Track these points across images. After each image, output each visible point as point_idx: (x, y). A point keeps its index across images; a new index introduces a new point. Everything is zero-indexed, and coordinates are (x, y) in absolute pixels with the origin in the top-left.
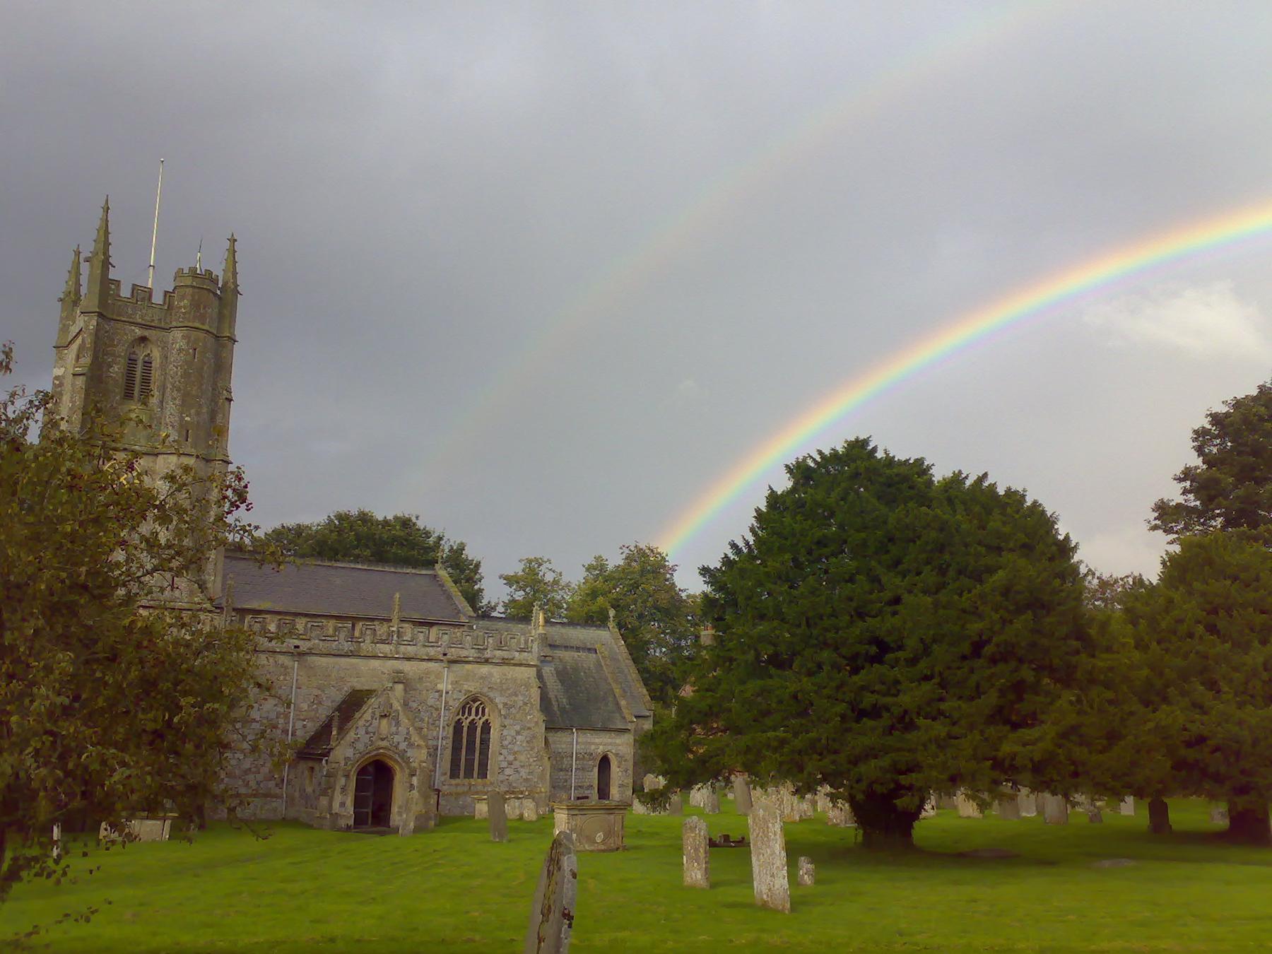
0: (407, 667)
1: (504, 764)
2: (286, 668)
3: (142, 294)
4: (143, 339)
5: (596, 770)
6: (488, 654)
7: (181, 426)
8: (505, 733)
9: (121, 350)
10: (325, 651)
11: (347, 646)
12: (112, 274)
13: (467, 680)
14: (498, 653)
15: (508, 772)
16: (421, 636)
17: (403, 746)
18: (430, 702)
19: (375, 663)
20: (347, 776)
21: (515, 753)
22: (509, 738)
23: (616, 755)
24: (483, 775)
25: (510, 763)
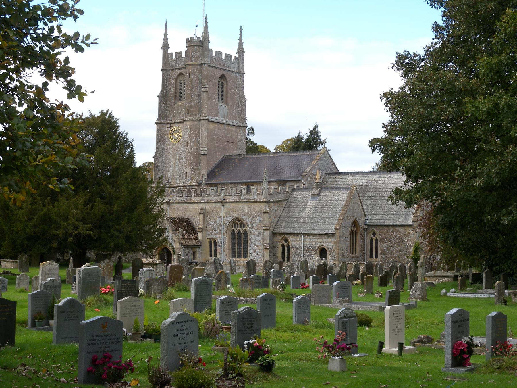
0: (208, 207)
1: (252, 251)
3: (179, 54)
4: (181, 74)
6: (243, 198)
8: (252, 236)
9: (173, 81)
12: (169, 51)
13: (232, 211)
14: (247, 197)
15: (254, 255)
16: (213, 192)
18: (218, 222)
19: (195, 205)
21: (257, 246)
22: (253, 238)
23: (329, 248)
24: (246, 256)
25: (255, 251)
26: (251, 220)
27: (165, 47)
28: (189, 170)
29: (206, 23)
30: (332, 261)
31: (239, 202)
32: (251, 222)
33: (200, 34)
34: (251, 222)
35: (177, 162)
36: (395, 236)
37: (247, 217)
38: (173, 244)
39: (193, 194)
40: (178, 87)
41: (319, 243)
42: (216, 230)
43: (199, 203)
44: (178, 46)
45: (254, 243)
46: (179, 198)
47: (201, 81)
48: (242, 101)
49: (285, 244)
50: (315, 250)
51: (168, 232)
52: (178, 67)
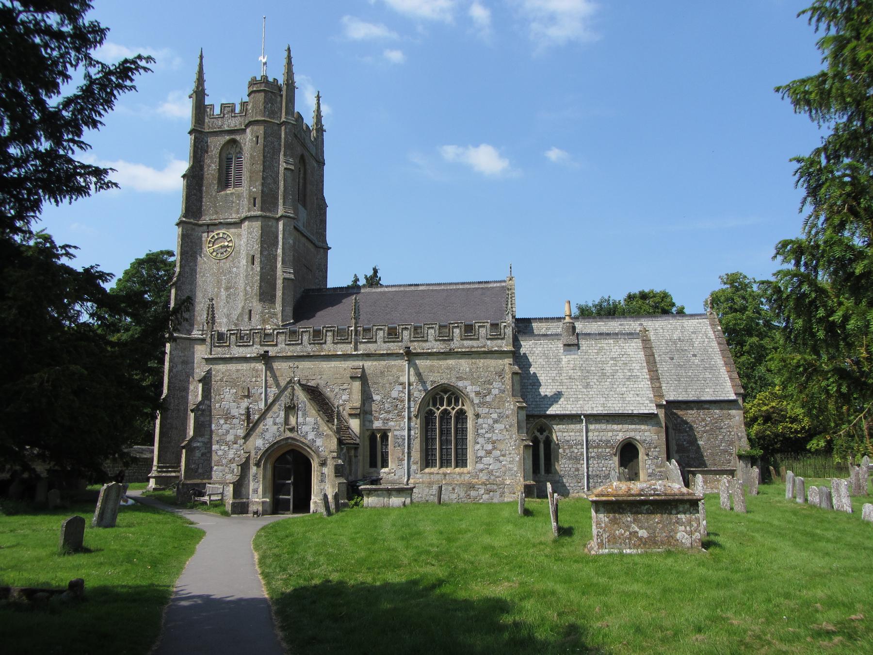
1: (481, 453)
2: (257, 371)
5: (616, 459)
6: (457, 344)
7: (250, 196)
8: (480, 421)
10: (289, 354)
11: (310, 349)
14: (467, 343)
15: (486, 460)
17: (311, 436)
18: (394, 394)
20: (258, 465)
21: (494, 442)
24: (461, 462)
25: (489, 453)
26: (478, 389)
27: (199, 94)
28: (257, 306)
29: (289, 58)
30: (654, 467)
31: (450, 354)
32: (478, 394)
33: (278, 75)
34: (478, 394)
35: (223, 293)
36: (704, 420)
37: (466, 383)
38: (319, 442)
39: (329, 339)
40: (225, 164)
41: (621, 434)
42: (389, 412)
43: (346, 357)
44: (228, 91)
45: (487, 435)
46: (292, 348)
47: (268, 157)
48: (322, 207)
49: (542, 438)
50: (612, 447)
51: (305, 415)
52: (227, 128)
